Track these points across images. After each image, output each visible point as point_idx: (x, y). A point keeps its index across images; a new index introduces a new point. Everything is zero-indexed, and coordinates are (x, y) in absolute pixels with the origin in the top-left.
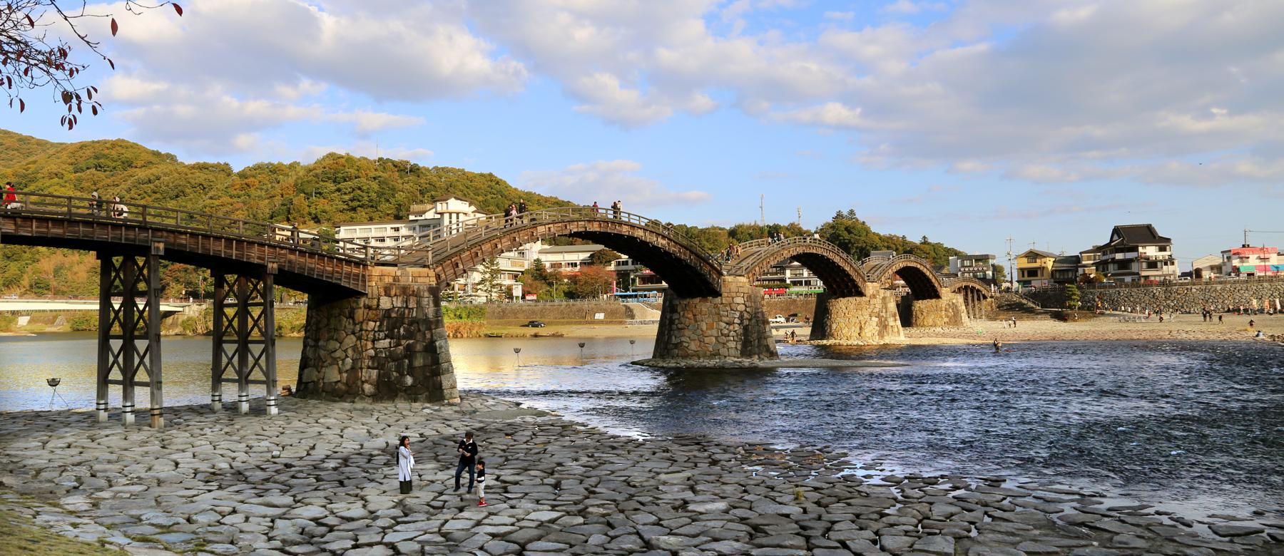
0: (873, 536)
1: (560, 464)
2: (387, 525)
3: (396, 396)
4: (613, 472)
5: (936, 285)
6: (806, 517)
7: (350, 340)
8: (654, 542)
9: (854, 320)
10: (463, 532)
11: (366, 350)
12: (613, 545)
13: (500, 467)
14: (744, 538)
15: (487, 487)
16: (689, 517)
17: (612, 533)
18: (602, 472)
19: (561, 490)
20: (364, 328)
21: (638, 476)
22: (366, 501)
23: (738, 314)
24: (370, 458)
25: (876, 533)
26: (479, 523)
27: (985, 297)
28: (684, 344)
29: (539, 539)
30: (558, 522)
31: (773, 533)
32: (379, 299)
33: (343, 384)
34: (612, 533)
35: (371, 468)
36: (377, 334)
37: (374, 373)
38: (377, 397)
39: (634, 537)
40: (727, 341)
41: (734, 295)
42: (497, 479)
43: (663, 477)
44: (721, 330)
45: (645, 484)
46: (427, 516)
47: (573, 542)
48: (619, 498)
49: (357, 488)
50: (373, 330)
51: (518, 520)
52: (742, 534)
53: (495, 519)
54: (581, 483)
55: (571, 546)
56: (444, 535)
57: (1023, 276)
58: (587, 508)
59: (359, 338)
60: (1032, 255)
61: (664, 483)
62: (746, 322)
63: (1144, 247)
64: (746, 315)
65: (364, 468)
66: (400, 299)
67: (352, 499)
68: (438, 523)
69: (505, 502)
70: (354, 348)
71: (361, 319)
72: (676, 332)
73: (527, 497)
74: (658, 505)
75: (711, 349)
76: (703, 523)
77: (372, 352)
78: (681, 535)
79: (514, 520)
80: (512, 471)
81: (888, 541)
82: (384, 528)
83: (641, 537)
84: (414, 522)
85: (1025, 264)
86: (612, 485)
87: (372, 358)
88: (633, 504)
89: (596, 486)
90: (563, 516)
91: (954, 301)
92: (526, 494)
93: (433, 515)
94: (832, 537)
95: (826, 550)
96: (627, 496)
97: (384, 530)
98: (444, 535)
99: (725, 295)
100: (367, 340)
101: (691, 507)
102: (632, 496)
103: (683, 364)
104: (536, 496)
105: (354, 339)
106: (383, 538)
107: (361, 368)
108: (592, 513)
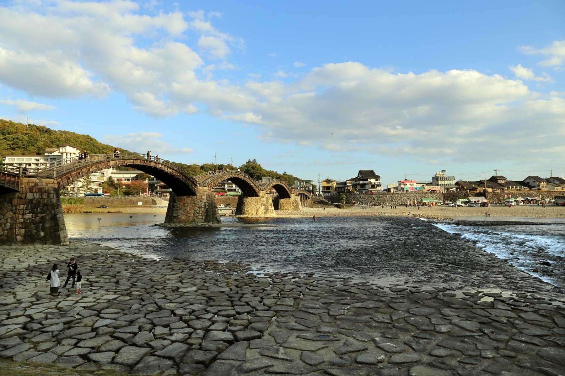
0: (260, 299)
1: (119, 272)
2: (27, 306)
3: (35, 241)
4: (144, 275)
5: (289, 192)
6: (231, 292)
7: (10, 214)
8: (163, 306)
9: (254, 207)
10: (69, 307)
11: (19, 219)
12: (144, 309)
13: (89, 274)
14: (204, 303)
15: (82, 284)
16: (179, 295)
17: (143, 303)
18: (139, 275)
19: (119, 284)
20: (18, 208)
21: (156, 277)
22: (16, 295)
23: (203, 203)
24: (19, 273)
25: (261, 298)
26: (77, 302)
27: (309, 198)
28: (179, 217)
29: (108, 308)
30: (117, 299)
31: (217, 300)
32: (26, 194)
33: (5, 236)
34: (143, 303)
35: (19, 278)
36: (25, 211)
37: (23, 231)
38: (24, 242)
39: (154, 305)
40: (199, 215)
41: (202, 195)
42: (87, 281)
43: (167, 277)
44: (196, 211)
45: (159, 280)
46: (49, 300)
47: (124, 309)
48: (147, 287)
49: (11, 288)
50: (23, 209)
51: (97, 300)
52: (203, 301)
53: (86, 300)
54: (129, 281)
55: (123, 310)
56: (58, 309)
57: (324, 190)
58: (131, 292)
59: (15, 213)
60: (328, 181)
61: (168, 280)
62: (207, 207)
63: (370, 179)
64: (207, 204)
65: (16, 278)
66: (38, 194)
67: (8, 294)
68: (55, 303)
69: (91, 291)
70: (12, 218)
71: (16, 204)
72: (175, 211)
73: (102, 288)
74: (165, 289)
75: (191, 219)
76: (186, 297)
77: (22, 220)
78: (175, 303)
79: (95, 299)
80: (95, 276)
81: (266, 301)
82: (25, 308)
83: (157, 305)
84: (42, 303)
85: (325, 184)
86: (144, 281)
87: (21, 223)
88: (154, 290)
89: (136, 282)
90: (120, 296)
91: (296, 199)
92: (102, 287)
93: (53, 299)
94: (243, 301)
95: (240, 306)
96: (151, 286)
97: (25, 309)
98: (58, 309)
99: (198, 195)
100: (19, 214)
101: (180, 290)
102: (153, 286)
103: (178, 226)
104: (106, 288)
105: (12, 214)
106: (24, 313)
107: (16, 228)
108: (133, 295)
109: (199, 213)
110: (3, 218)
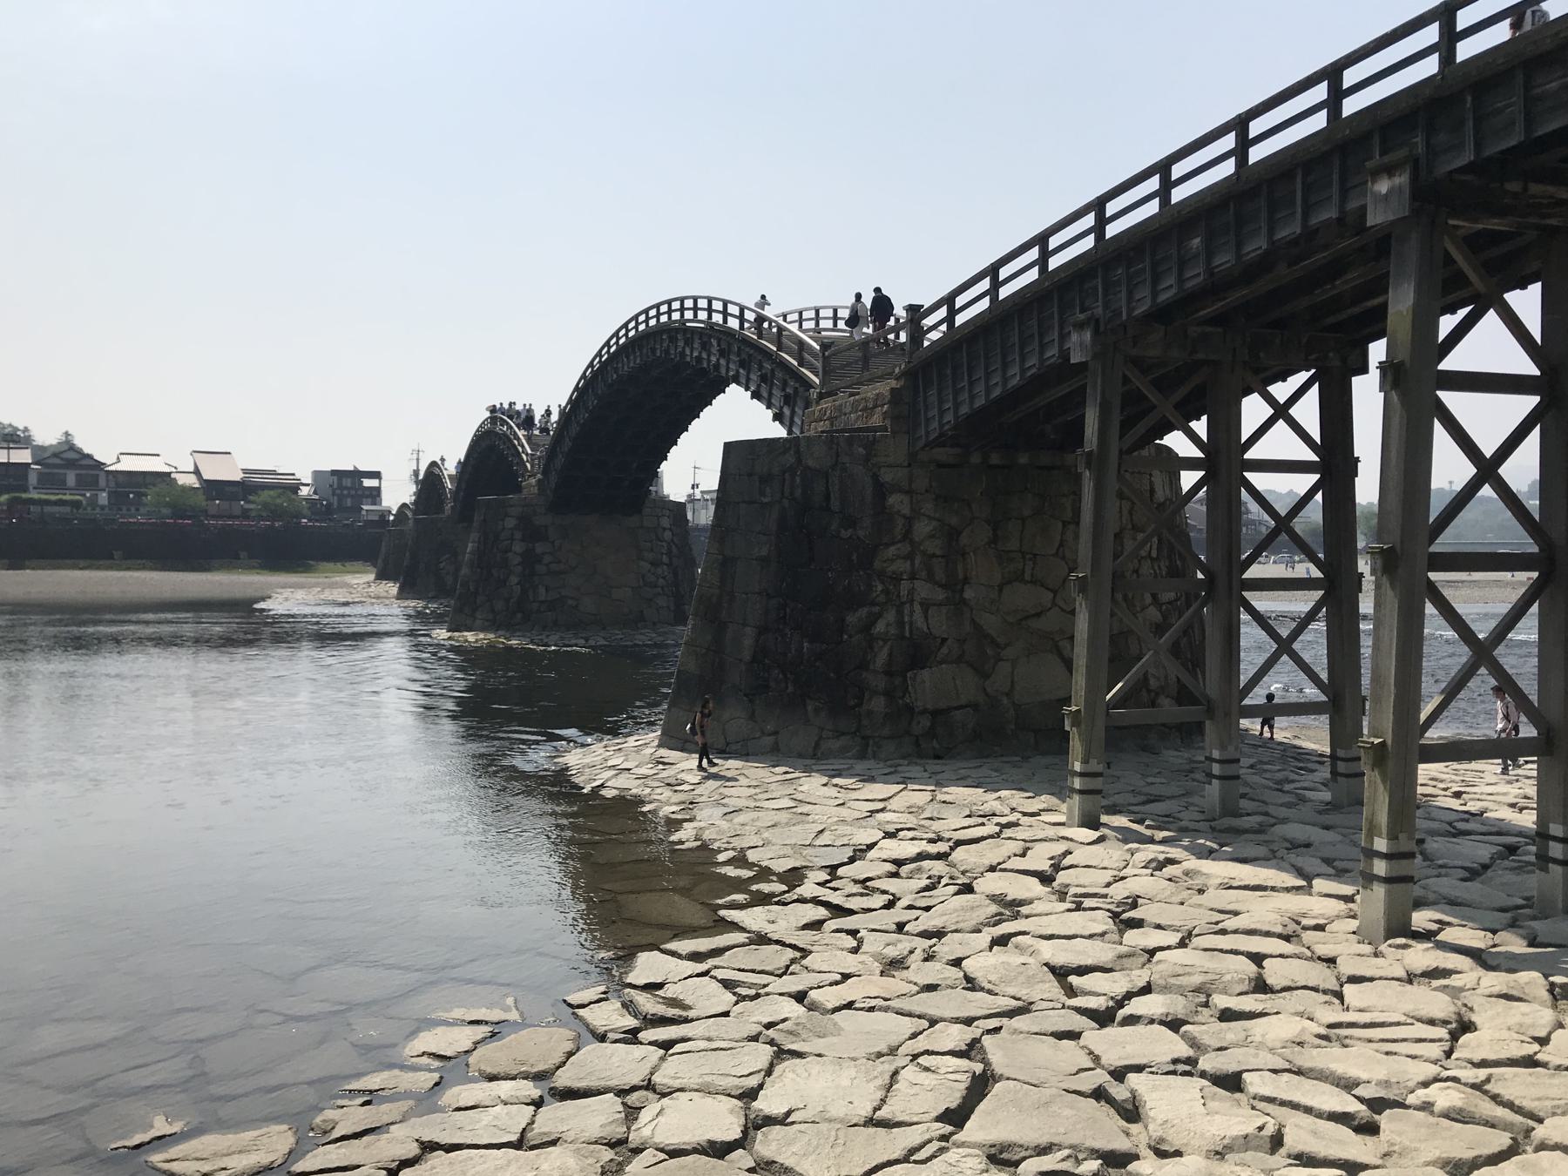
28: (570, 602)
109: (656, 586)
110: (1054, 604)
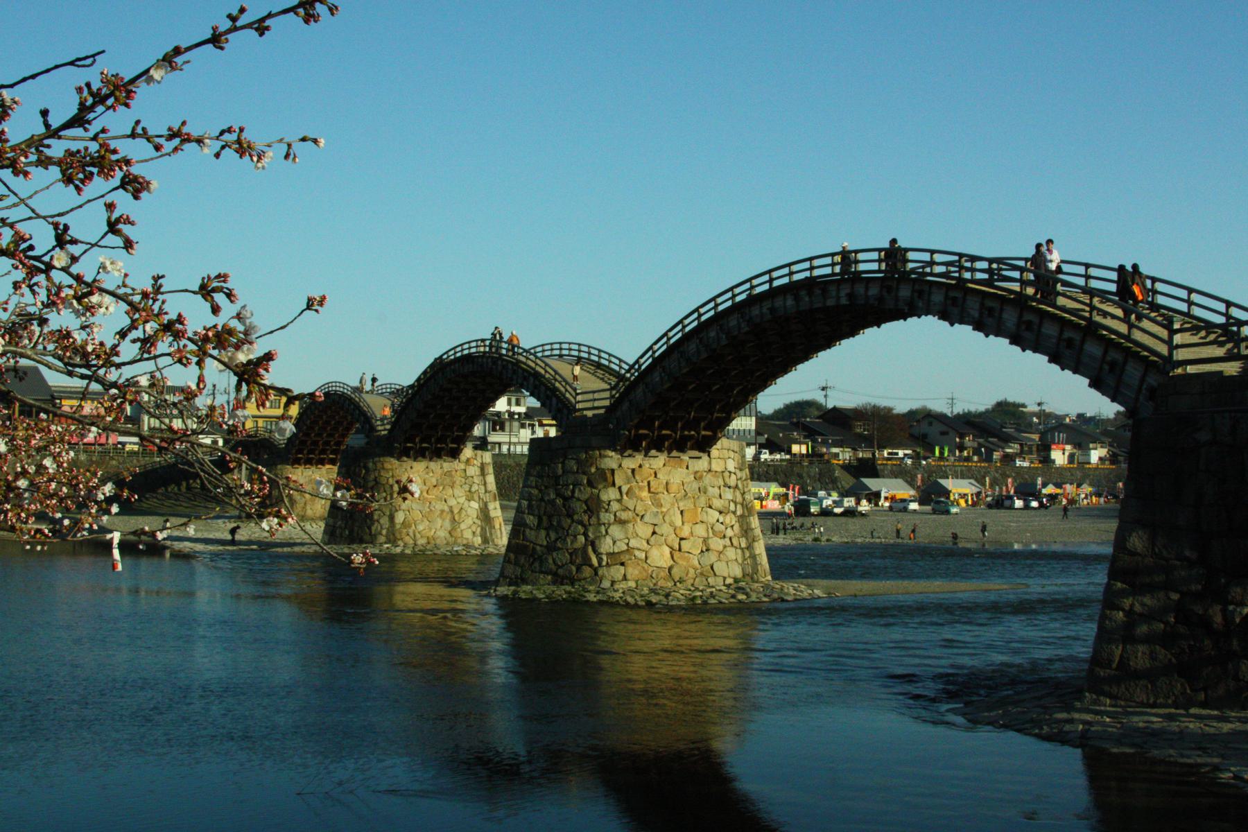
28: (637, 553)
72: (615, 531)
109: (724, 537)
